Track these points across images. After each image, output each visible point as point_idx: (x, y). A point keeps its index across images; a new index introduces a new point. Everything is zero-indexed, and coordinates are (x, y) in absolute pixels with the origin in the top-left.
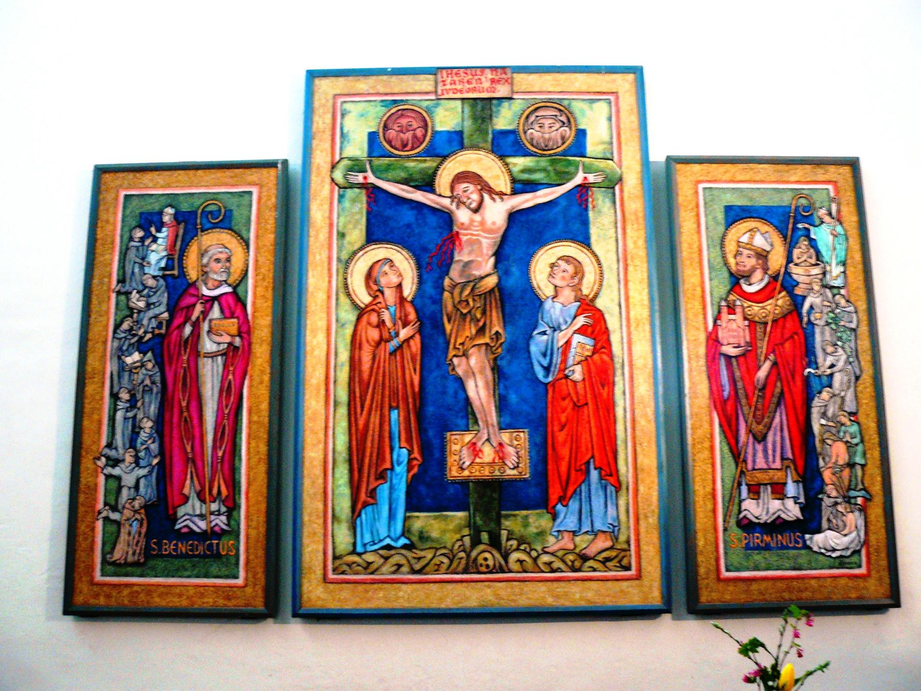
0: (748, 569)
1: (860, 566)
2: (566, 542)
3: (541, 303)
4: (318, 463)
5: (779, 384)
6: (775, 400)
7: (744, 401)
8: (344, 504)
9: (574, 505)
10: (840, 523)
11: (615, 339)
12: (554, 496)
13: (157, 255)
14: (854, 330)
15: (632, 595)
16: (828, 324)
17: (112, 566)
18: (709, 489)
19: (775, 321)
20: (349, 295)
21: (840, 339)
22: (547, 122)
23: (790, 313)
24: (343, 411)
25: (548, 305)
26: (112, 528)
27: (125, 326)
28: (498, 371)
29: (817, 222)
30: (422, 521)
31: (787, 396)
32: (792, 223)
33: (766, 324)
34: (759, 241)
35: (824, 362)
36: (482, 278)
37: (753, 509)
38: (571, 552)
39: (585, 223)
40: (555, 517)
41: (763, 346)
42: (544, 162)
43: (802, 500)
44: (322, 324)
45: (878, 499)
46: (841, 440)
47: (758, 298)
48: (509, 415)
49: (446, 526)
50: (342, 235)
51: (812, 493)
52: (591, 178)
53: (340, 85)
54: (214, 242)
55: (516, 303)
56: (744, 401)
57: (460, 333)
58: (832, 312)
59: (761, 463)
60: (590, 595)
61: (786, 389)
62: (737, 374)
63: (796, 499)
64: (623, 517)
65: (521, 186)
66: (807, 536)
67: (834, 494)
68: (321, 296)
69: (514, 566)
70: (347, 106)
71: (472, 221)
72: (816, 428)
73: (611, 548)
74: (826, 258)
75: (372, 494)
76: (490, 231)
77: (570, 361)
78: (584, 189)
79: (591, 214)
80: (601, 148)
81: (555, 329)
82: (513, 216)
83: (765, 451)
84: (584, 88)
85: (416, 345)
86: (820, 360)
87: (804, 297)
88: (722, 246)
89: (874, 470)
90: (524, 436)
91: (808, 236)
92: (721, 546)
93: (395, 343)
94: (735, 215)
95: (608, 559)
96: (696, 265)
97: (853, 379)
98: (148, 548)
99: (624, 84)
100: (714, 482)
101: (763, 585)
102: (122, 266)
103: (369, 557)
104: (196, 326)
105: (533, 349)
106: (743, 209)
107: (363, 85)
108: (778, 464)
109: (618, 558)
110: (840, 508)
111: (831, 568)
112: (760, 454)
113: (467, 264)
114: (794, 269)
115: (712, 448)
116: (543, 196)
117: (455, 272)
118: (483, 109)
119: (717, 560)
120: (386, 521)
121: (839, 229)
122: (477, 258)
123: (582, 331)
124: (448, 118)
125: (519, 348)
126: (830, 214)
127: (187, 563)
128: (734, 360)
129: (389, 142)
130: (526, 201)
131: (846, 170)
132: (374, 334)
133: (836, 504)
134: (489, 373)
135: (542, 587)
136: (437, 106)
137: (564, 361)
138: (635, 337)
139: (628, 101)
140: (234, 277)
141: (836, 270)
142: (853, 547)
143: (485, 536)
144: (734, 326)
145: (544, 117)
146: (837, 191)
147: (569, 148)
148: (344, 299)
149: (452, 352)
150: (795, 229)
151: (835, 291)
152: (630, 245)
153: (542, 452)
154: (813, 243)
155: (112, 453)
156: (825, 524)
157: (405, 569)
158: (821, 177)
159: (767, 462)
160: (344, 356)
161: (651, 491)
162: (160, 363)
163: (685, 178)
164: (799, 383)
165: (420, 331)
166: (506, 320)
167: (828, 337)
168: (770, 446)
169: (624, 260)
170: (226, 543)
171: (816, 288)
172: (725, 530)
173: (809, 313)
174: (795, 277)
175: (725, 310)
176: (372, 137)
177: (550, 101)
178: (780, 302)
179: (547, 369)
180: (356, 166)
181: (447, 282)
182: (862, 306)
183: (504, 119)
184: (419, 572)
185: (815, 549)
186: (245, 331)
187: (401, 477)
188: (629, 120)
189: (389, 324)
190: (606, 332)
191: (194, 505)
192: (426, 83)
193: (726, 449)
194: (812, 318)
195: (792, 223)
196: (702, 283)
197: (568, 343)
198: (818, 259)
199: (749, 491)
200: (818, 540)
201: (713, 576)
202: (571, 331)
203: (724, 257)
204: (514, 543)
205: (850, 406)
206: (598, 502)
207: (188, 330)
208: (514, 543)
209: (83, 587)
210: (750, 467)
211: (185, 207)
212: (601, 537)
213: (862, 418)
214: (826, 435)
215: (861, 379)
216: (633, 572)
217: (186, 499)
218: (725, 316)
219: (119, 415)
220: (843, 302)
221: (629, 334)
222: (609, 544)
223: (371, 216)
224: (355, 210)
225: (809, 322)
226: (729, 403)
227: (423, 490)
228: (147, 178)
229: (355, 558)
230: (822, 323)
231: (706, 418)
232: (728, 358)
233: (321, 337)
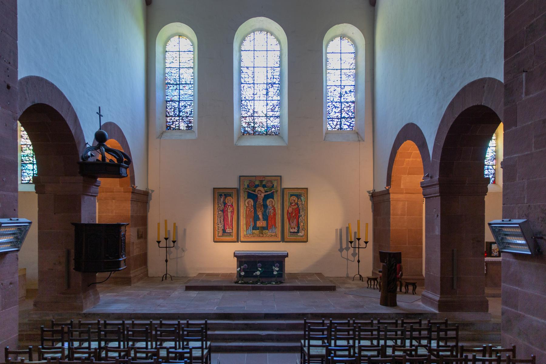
13: (222, 200)
15: (277, 240)
17: (220, 236)
28: (263, 215)
30: (254, 231)
32: (298, 196)
37: (291, 230)
48: (264, 219)
49: (257, 232)
53: (244, 178)
54: (229, 198)
55: (265, 206)
57: (258, 210)
65: (266, 192)
78: (273, 193)
82: (265, 195)
94: (292, 195)
99: (279, 178)
107: (246, 178)
109: (276, 236)
116: (269, 193)
118: (261, 181)
120: (250, 231)
122: (260, 201)
124: (257, 183)
125: (265, 211)
130: (266, 193)
139: (279, 181)
163: (285, 191)
169: (278, 201)
183: (264, 183)
186: (233, 209)
188: (279, 183)
191: (228, 229)
192: (254, 178)
195: (298, 196)
223: (248, 196)
224: (246, 194)
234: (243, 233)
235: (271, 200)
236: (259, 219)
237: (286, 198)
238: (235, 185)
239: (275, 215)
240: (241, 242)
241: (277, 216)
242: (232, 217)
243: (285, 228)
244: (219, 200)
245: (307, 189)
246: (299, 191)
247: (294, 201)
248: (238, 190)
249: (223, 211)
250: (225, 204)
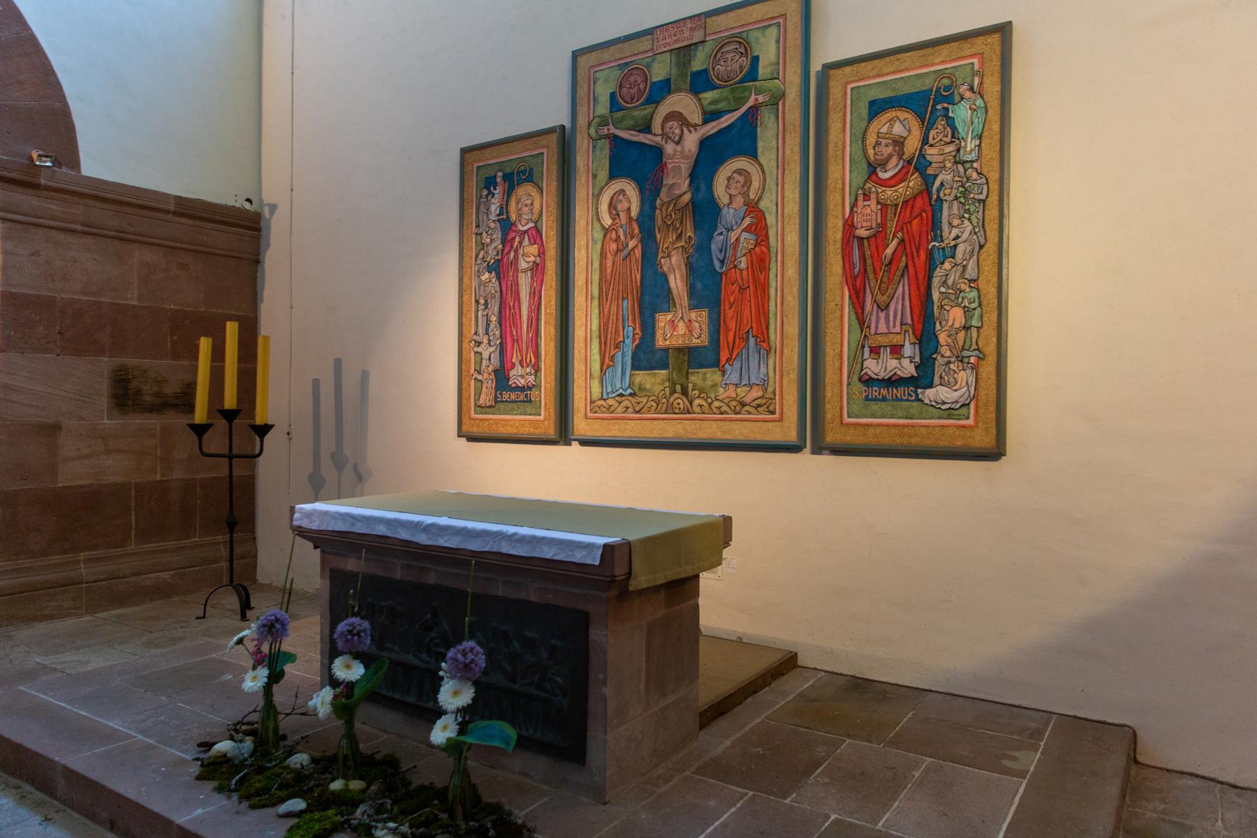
0: (866, 417)
1: (968, 418)
2: (731, 392)
3: (720, 210)
4: (582, 339)
5: (904, 259)
6: (899, 273)
7: (871, 276)
8: (596, 367)
9: (737, 365)
10: (952, 380)
11: (772, 233)
12: (723, 359)
13: (494, 208)
14: (984, 201)
15: (775, 433)
16: (956, 198)
17: (481, 408)
18: (837, 351)
19: (905, 203)
20: (599, 220)
21: (968, 211)
22: (729, 56)
23: (921, 192)
24: (596, 302)
25: (724, 211)
26: (479, 384)
27: (481, 256)
28: (690, 267)
29: (957, 98)
30: (642, 377)
31: (911, 269)
32: (930, 105)
33: (897, 205)
34: (898, 129)
35: (949, 234)
36: (681, 196)
37: (873, 367)
38: (734, 399)
39: (754, 139)
40: (724, 373)
41: (892, 226)
42: (726, 92)
43: (917, 359)
44: (584, 242)
45: (992, 358)
46: (959, 305)
47: (892, 182)
48: (697, 300)
49: (654, 380)
50: (595, 176)
51: (926, 354)
52: (761, 99)
53: (593, 58)
55: (704, 212)
56: (871, 276)
57: (665, 239)
58: (963, 186)
59: (882, 328)
60: (746, 431)
61: (910, 263)
62: (868, 253)
63: (911, 359)
64: (771, 373)
65: (710, 116)
66: (919, 391)
67: (948, 353)
68: (583, 222)
69: (697, 409)
70: (598, 75)
71: (675, 151)
72: (935, 296)
73: (762, 397)
74: (962, 133)
75: (612, 358)
76: (686, 158)
77: (739, 255)
78: (755, 109)
79: (759, 130)
80: (770, 69)
81: (730, 229)
82: (703, 143)
83: (887, 318)
84: (760, 18)
85: (638, 253)
86: (945, 234)
87: (936, 176)
88: (864, 139)
89: (989, 331)
90: (705, 313)
91: (947, 116)
92: (845, 397)
93: (626, 252)
94: (877, 108)
95: (759, 406)
96: (840, 161)
97: (977, 248)
98: (496, 397)
100: (842, 346)
101: (878, 430)
102: (477, 217)
103: (610, 402)
104: (516, 252)
105: (713, 247)
106: (885, 101)
107: (605, 55)
108: (897, 329)
109: (766, 406)
110: (952, 366)
111: (939, 418)
112: (882, 321)
113: (672, 187)
114: (929, 151)
115: (842, 317)
117: (664, 196)
119: (841, 408)
121: (979, 102)
122: (678, 182)
123: (748, 229)
124: (659, 72)
125: (703, 248)
126: (971, 89)
127: (514, 405)
128: (865, 242)
129: (623, 98)
130: (713, 128)
131: (995, 39)
132: (614, 246)
133: (949, 362)
134: (683, 268)
135: (714, 425)
136: (653, 61)
137: (734, 255)
138: (787, 230)
140: (535, 217)
141: (970, 144)
142: (962, 401)
143: (678, 388)
144: (868, 211)
145: (728, 52)
146: (982, 63)
147: (746, 75)
148: (596, 223)
149: (660, 255)
150: (934, 110)
151: (968, 165)
152: (788, 152)
154: (950, 122)
155: (477, 338)
156: (937, 380)
157: (630, 410)
158: (967, 52)
159: (888, 327)
160: (596, 264)
161: (792, 353)
162: (499, 279)
164: (923, 256)
165: (641, 242)
166: (696, 227)
167: (955, 210)
168: (891, 314)
169: (782, 166)
170: (534, 392)
171: (948, 165)
172: (849, 384)
173: (938, 191)
174: (928, 157)
175: (861, 197)
176: (613, 95)
177: (733, 36)
178: (911, 184)
179: (722, 262)
180: (604, 122)
181: (658, 202)
182: (994, 177)
183: (697, 65)
184: (638, 412)
185: (927, 401)
186: (542, 253)
188: (794, 36)
189: (622, 238)
190: (766, 227)
192: (645, 44)
193: (854, 317)
194: (942, 195)
195: (930, 105)
196: (843, 174)
197: (738, 240)
198: (953, 137)
199: (871, 352)
200: (929, 394)
201: (837, 421)
202: (740, 230)
203: (864, 150)
204: (697, 392)
205: (971, 272)
206: (753, 363)
207: (512, 254)
208: (697, 392)
209: (465, 420)
210: (873, 331)
211: (508, 171)
212: (755, 388)
213: (981, 283)
214: (945, 301)
215: (985, 249)
216: (777, 416)
217: (513, 366)
218: (860, 203)
219: (480, 313)
220: (975, 175)
221: (783, 228)
222: (760, 394)
225: (939, 199)
226: (858, 280)
227: (642, 356)
228: (487, 152)
229: (602, 402)
230: (951, 198)
231: (838, 293)
232: (861, 239)
233: (584, 252)
234: (584, 389)
235: (741, 163)
236: (665, 299)
237: (841, 134)
238: (552, 111)
239: (761, 263)
240: (584, 443)
241: (774, 269)
242: (536, 295)
243: (830, 351)
244: (483, 205)
245: (1003, 31)
246: (940, 63)
247: (899, 143)
248: (564, 140)
249: (501, 268)
250: (507, 226)
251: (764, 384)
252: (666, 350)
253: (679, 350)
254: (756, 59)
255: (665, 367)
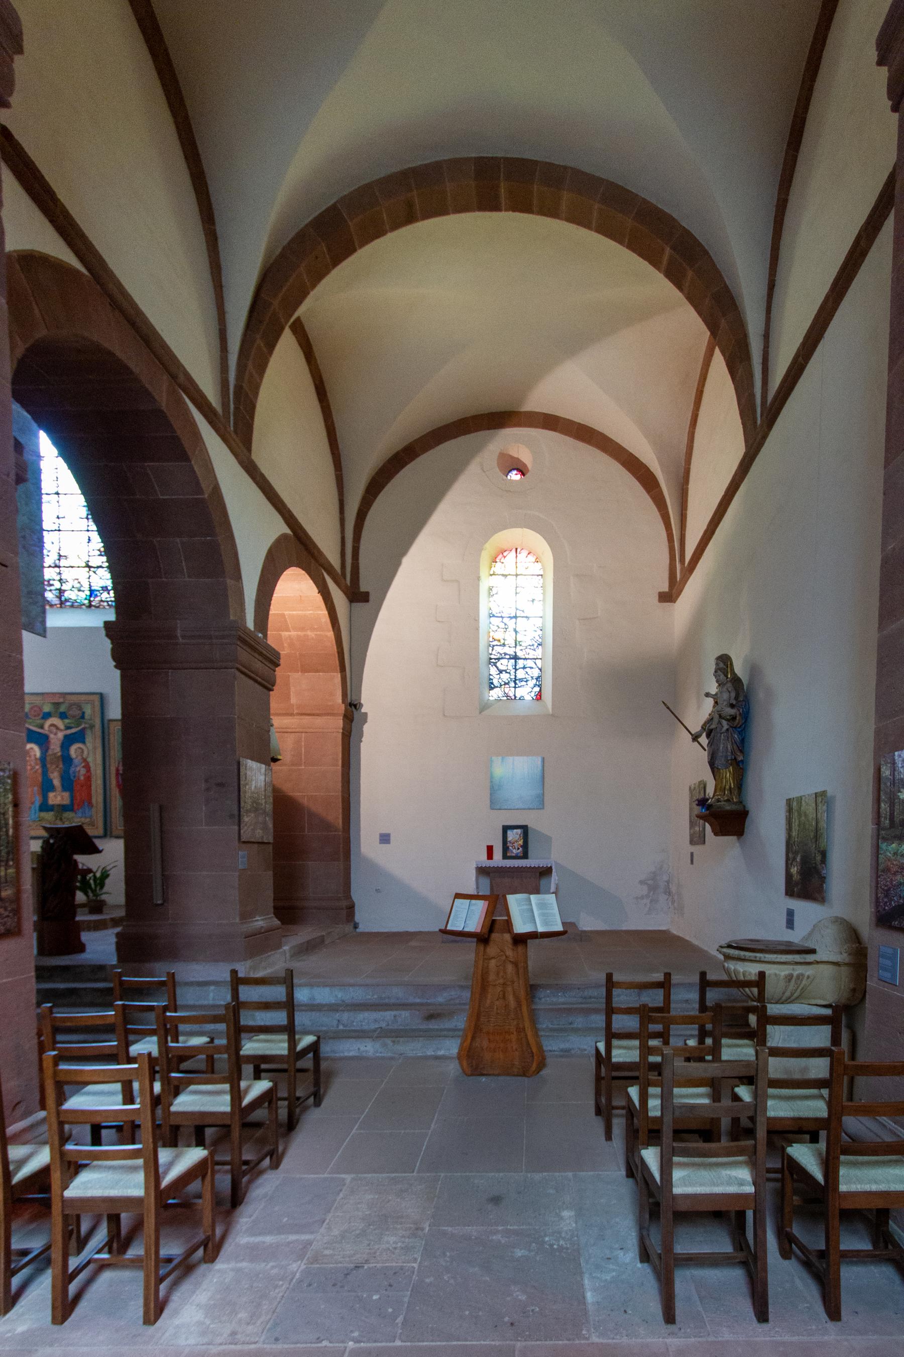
30: (43, 814)
48: (65, 788)
55: (67, 760)
65: (68, 728)
78: (83, 730)
82: (66, 736)
85: (40, 771)
99: (97, 699)
116: (73, 731)
117: (50, 752)
124: (47, 709)
130: (69, 732)
153: (73, 798)
166: (64, 764)
183: (62, 709)
187: (37, 804)
192: (40, 698)
236: (52, 788)
239: (88, 778)
241: (93, 780)
251: (91, 817)
252: (53, 806)
253: (59, 805)
254: (84, 713)
255: (52, 810)
